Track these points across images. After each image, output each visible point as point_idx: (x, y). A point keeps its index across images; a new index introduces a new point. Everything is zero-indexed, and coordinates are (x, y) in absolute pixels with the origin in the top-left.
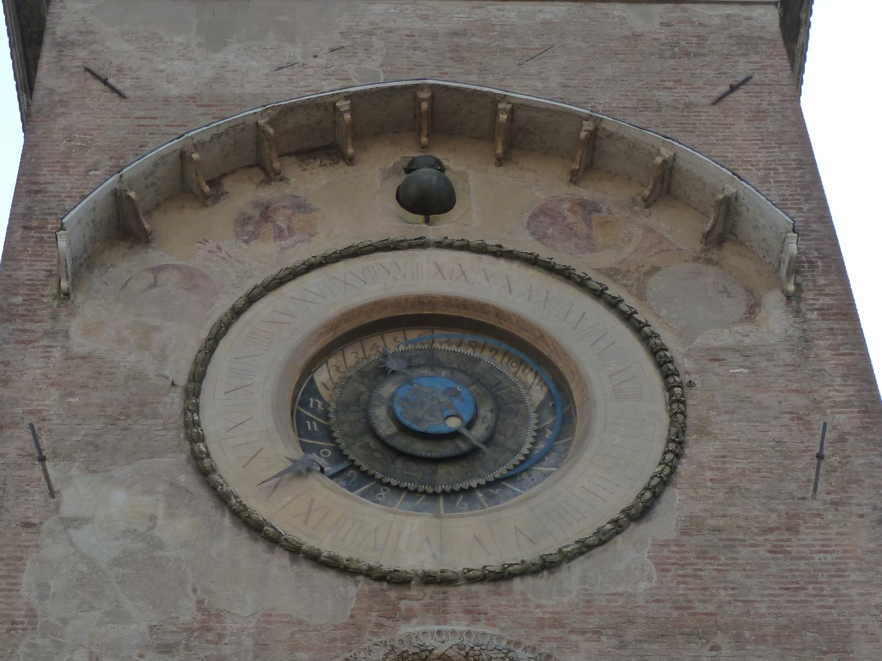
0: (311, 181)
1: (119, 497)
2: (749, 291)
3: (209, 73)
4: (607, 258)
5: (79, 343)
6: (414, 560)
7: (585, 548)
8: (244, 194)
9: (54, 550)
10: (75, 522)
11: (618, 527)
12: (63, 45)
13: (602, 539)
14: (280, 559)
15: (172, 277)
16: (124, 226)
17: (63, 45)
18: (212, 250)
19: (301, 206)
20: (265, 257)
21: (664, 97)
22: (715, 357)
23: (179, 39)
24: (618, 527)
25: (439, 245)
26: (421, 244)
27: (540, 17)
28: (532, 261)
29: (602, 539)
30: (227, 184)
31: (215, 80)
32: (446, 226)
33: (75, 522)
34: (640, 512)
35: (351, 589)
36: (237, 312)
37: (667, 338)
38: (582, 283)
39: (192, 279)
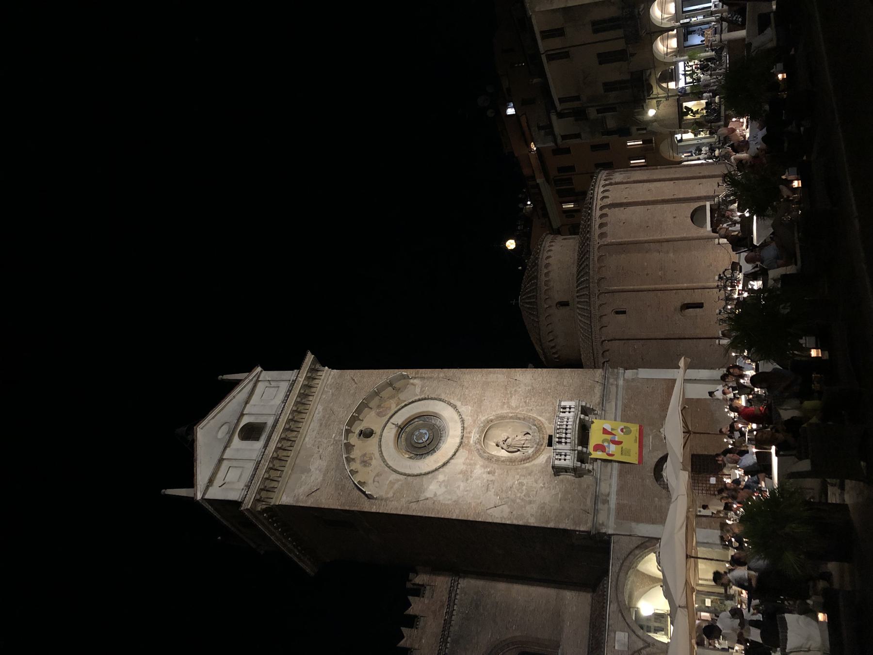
0: (356, 454)
1: (431, 487)
5: (390, 495)
6: (458, 440)
9: (441, 498)
10: (435, 495)
12: (297, 501)
14: (452, 461)
15: (376, 479)
17: (297, 501)
19: (365, 455)
22: (422, 392)
23: (304, 477)
26: (381, 435)
31: (320, 471)
32: (378, 430)
33: (435, 495)
35: (461, 450)
37: (417, 398)
39: (378, 475)
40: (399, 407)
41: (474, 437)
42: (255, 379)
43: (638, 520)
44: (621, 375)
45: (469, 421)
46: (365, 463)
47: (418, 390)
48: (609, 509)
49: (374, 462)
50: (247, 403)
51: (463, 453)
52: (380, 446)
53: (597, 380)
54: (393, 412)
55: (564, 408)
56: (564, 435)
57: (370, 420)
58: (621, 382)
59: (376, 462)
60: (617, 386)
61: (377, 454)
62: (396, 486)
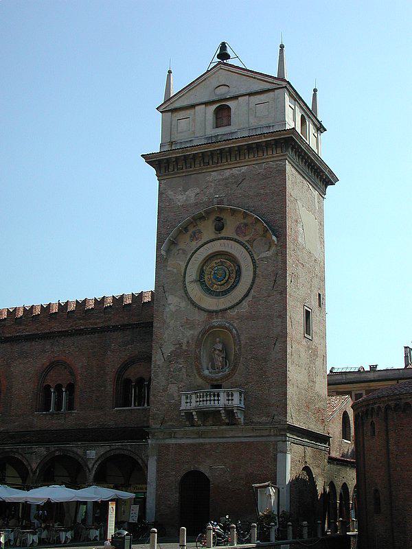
2: (270, 243)
3: (185, 199)
4: (247, 238)
5: (168, 269)
7: (238, 304)
8: (191, 230)
9: (167, 310)
10: (169, 304)
11: (243, 299)
13: (241, 301)
16: (173, 243)
18: (187, 244)
19: (200, 232)
20: (195, 244)
21: (262, 191)
22: (262, 259)
24: (243, 299)
25: (222, 238)
27: (243, 171)
28: (235, 240)
29: (241, 301)
30: (189, 228)
33: (169, 304)
34: (246, 295)
36: (190, 259)
38: (242, 245)
39: (184, 252)
40: (247, 244)
41: (216, 321)
42: (275, 86)
43: (158, 461)
44: (279, 438)
45: (233, 313)
46: (194, 237)
47: (264, 255)
48: (164, 439)
49: (194, 243)
50: (250, 94)
51: (204, 316)
52: (205, 243)
53: (276, 417)
54: (240, 239)
55: (232, 396)
56: (201, 399)
57: (231, 225)
58: (273, 439)
59: (195, 244)
60: (268, 436)
61: (200, 243)
62: (175, 270)
